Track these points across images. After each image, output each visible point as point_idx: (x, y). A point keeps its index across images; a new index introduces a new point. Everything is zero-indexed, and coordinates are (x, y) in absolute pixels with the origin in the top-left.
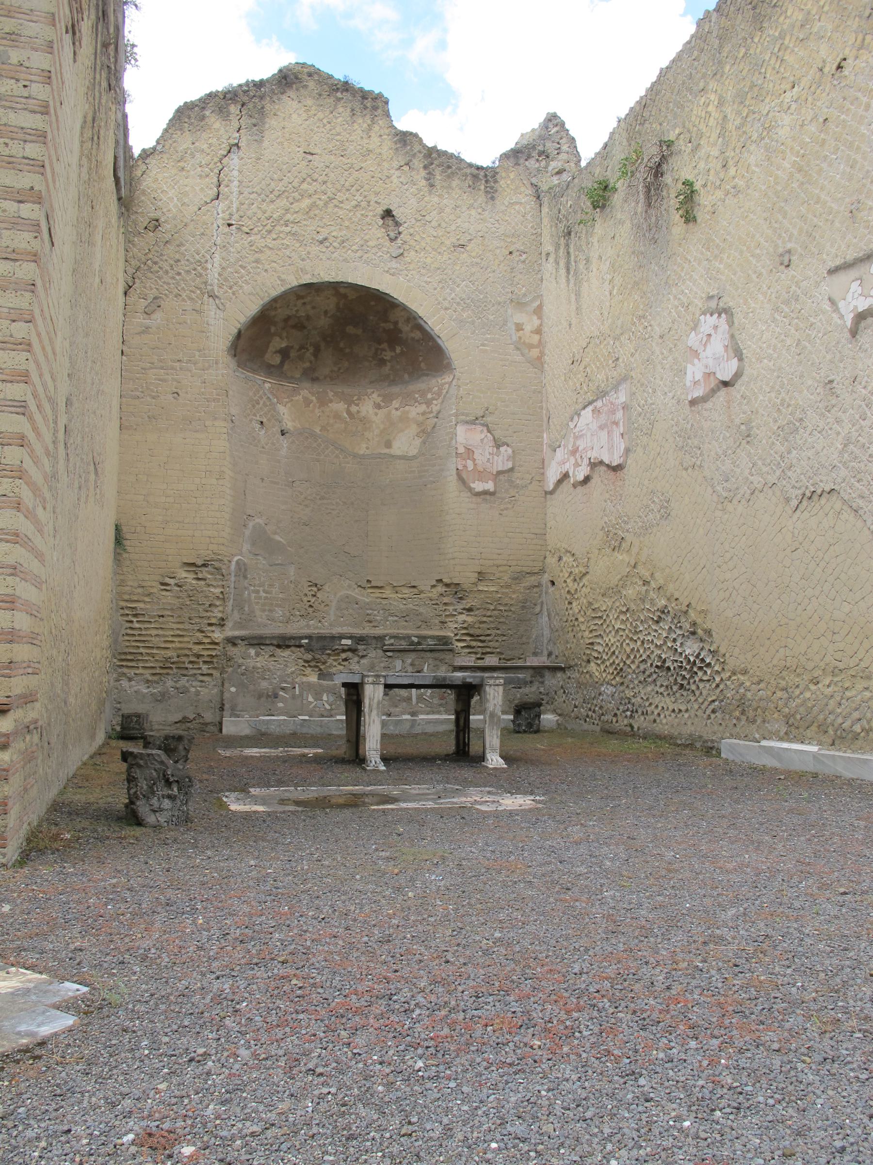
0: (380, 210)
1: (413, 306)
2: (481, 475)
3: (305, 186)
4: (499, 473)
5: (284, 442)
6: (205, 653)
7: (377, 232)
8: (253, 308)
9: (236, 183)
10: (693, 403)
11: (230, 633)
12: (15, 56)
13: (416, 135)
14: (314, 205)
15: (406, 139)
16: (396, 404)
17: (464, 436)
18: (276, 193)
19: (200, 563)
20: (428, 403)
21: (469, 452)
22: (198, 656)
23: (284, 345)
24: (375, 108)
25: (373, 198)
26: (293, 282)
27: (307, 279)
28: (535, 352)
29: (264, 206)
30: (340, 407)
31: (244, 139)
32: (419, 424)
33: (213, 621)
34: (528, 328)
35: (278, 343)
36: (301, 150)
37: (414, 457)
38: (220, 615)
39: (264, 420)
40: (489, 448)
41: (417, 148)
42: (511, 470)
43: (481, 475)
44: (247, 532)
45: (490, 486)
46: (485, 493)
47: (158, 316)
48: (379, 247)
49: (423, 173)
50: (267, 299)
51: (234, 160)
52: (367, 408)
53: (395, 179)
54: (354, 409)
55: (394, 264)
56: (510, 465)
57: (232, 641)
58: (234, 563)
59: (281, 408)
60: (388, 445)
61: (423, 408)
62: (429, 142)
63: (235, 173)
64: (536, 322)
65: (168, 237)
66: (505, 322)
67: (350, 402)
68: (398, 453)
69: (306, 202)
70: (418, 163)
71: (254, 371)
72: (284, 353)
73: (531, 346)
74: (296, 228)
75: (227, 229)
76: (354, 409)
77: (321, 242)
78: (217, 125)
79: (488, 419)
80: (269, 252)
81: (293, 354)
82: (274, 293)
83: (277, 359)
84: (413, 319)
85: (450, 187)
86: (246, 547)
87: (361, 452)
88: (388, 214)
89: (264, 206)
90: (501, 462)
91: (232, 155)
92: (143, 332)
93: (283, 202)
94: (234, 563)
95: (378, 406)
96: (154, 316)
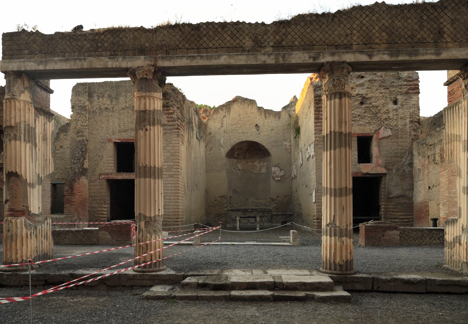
0: (255, 125)
1: (262, 144)
2: (277, 177)
3: (239, 122)
4: (281, 176)
5: (239, 172)
7: (254, 130)
8: (230, 148)
10: (300, 167)
12: (176, 154)
13: (262, 107)
14: (241, 126)
15: (260, 108)
16: (262, 162)
17: (273, 169)
20: (268, 162)
21: (275, 172)
23: (238, 153)
24: (253, 103)
25: (253, 122)
26: (237, 142)
27: (240, 141)
28: (289, 150)
30: (251, 164)
32: (266, 166)
34: (288, 145)
35: (236, 153)
37: (265, 173)
40: (279, 171)
41: (262, 110)
42: (284, 175)
43: (277, 177)
44: (232, 190)
45: (279, 179)
46: (278, 180)
47: (212, 151)
48: (255, 132)
49: (264, 115)
51: (225, 119)
52: (256, 163)
53: (258, 118)
54: (254, 164)
55: (258, 136)
56: (284, 174)
59: (238, 165)
60: (261, 171)
61: (267, 163)
62: (265, 108)
64: (290, 144)
66: (283, 145)
67: (253, 162)
68: (263, 172)
69: (240, 125)
70: (263, 113)
71: (232, 159)
72: (238, 154)
73: (288, 149)
74: (238, 131)
76: (254, 164)
77: (243, 133)
79: (279, 165)
81: (240, 154)
82: (234, 144)
83: (237, 156)
84: (262, 146)
85: (270, 117)
86: (231, 193)
87: (255, 172)
88: (257, 125)
89: (231, 127)
90: (282, 173)
95: (258, 163)
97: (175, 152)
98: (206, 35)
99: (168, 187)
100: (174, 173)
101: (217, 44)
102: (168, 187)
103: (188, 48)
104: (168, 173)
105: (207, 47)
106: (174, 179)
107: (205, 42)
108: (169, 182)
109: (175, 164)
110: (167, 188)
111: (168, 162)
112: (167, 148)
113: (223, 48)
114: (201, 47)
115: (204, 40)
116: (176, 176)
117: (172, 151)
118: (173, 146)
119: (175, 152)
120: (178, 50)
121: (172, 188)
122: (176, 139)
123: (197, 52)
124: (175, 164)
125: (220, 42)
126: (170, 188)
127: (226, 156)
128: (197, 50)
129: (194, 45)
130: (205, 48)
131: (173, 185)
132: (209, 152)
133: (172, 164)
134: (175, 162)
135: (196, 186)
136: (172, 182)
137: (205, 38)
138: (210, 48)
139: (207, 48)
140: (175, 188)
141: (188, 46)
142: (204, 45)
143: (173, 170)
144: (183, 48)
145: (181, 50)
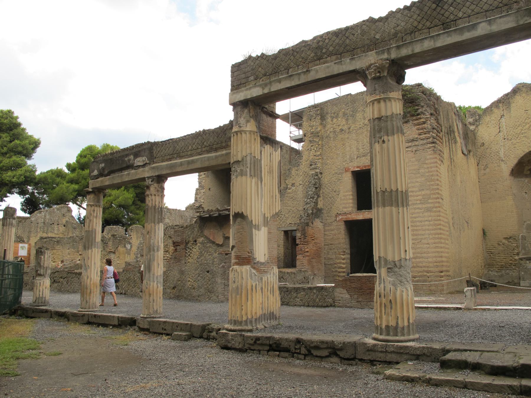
3: (526, 121)
6: (513, 263)
8: (515, 161)
9: (505, 126)
11: (521, 257)
12: (433, 178)
18: (518, 126)
19: (509, 237)
22: (511, 264)
29: (514, 131)
31: (505, 113)
33: (515, 254)
36: (524, 110)
38: (517, 252)
39: (527, 192)
44: (524, 226)
47: (488, 170)
50: (519, 158)
51: (503, 120)
57: (521, 259)
58: (520, 236)
63: (504, 123)
65: (487, 147)
71: (521, 178)
74: (525, 134)
75: (504, 140)
78: (496, 111)
80: (518, 144)
82: (521, 156)
86: (524, 231)
89: (514, 131)
91: (502, 118)
92: (484, 175)
93: (519, 128)
94: (520, 236)
96: (486, 170)
97: (432, 175)
98: (452, 4)
99: (425, 225)
100: (432, 205)
101: (470, 11)
102: (425, 225)
103: (430, 27)
104: (424, 206)
105: (456, 18)
106: (432, 214)
107: (451, 13)
108: (426, 219)
109: (432, 192)
110: (424, 228)
111: (423, 190)
112: (420, 171)
113: (478, 13)
114: (448, 20)
115: (450, 10)
116: (435, 209)
117: (427, 174)
118: (428, 168)
119: (432, 175)
120: (417, 33)
121: (431, 227)
122: (431, 156)
123: (442, 29)
124: (432, 192)
125: (473, 7)
126: (427, 227)
127: (510, 175)
128: (442, 26)
129: (438, 21)
130: (453, 21)
131: (431, 223)
132: (483, 172)
133: (428, 192)
134: (433, 189)
135: (467, 223)
136: (430, 218)
137: (451, 8)
138: (460, 18)
139: (455, 20)
140: (435, 227)
141: (430, 24)
142: (452, 17)
143: (430, 201)
144: (424, 28)
145: (421, 32)
